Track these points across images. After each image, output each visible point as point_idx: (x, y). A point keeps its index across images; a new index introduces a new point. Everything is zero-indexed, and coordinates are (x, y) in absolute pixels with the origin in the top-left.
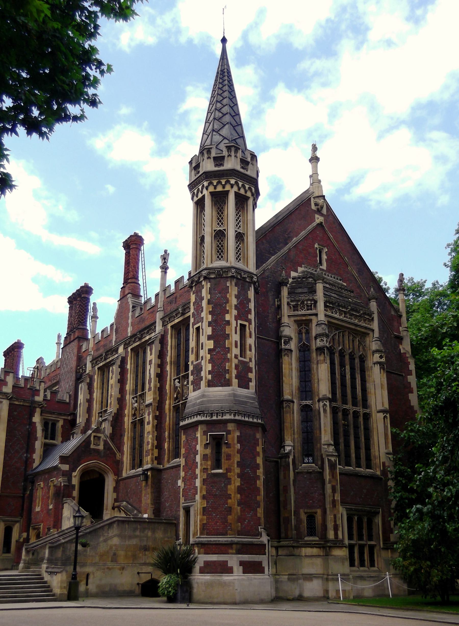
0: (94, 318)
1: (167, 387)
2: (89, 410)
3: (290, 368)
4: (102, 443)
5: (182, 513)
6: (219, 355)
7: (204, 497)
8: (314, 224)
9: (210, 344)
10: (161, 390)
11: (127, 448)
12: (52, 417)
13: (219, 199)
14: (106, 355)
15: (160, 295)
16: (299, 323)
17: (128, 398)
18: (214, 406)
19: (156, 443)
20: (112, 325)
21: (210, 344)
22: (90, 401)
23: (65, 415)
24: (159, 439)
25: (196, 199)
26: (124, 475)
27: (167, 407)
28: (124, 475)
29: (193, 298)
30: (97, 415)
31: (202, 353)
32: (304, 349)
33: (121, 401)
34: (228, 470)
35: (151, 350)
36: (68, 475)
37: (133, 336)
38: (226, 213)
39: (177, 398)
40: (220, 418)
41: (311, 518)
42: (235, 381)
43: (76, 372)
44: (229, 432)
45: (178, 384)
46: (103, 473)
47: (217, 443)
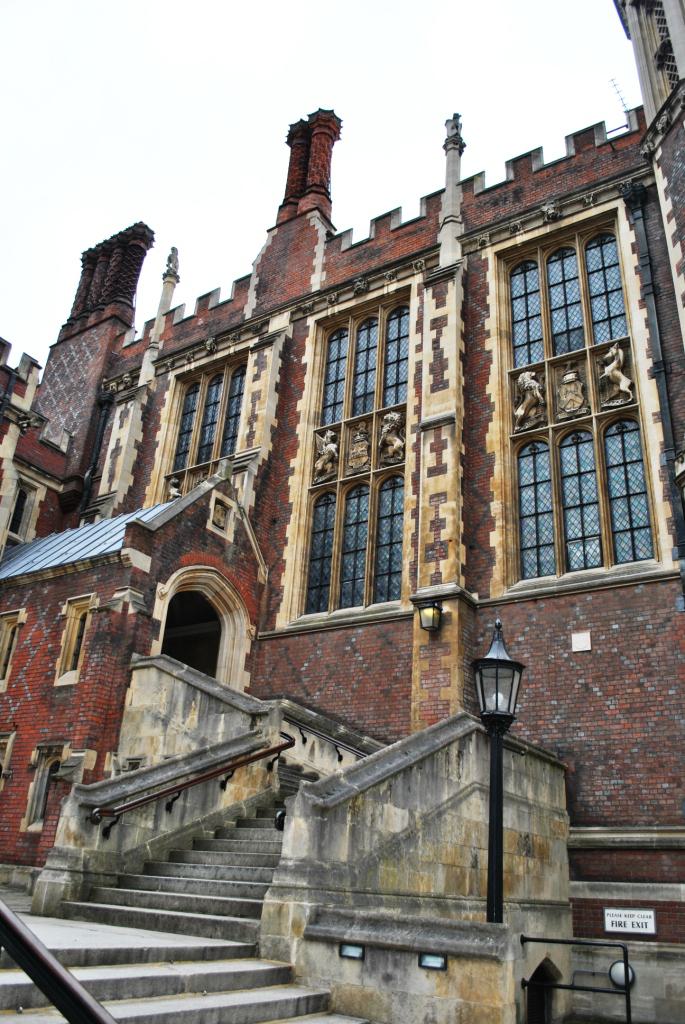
0: (171, 276)
2: (141, 469)
4: (231, 526)
11: (294, 553)
14: (216, 343)
15: (444, 197)
17: (304, 431)
22: (145, 449)
23: (53, 478)
26: (282, 622)
28: (282, 622)
30: (163, 481)
36: (146, 585)
37: (330, 292)
43: (99, 388)
46: (220, 608)
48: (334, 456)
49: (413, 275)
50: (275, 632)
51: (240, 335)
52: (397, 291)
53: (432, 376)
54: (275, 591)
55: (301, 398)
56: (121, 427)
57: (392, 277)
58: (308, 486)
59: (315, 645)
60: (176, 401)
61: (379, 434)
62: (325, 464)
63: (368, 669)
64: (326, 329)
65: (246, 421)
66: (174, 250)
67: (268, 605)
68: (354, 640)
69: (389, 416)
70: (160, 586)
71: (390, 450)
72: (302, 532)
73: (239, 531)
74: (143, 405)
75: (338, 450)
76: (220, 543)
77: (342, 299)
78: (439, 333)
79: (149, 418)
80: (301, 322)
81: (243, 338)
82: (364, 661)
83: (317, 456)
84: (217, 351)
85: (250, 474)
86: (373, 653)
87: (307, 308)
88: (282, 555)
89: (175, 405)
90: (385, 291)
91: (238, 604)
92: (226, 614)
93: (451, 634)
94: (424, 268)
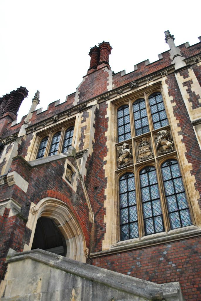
0: (36, 99)
14: (58, 117)
17: (110, 145)
26: (107, 245)
28: (107, 245)
36: (25, 201)
46: (67, 234)
48: (129, 154)
49: (162, 77)
50: (103, 252)
51: (71, 113)
52: (154, 85)
53: (191, 103)
54: (100, 227)
55: (107, 131)
56: (7, 153)
57: (150, 80)
58: (115, 169)
59: (135, 259)
60: (36, 144)
61: (156, 143)
62: (124, 159)
63: (182, 273)
64: (116, 105)
65: (79, 139)
66: (38, 91)
67: (96, 235)
68: (165, 253)
69: (161, 132)
70: (33, 205)
71: (164, 147)
72: (114, 193)
73: (79, 187)
74: (19, 145)
75: (131, 152)
76: (70, 190)
77: (124, 92)
78: (189, 87)
80: (103, 103)
81: (72, 114)
82: (177, 267)
83: (118, 154)
84: (59, 121)
85: (84, 159)
86: (183, 261)
87: (106, 97)
88: (103, 205)
89: (35, 145)
90: (147, 85)
91: (79, 232)
92: (70, 238)
94: (167, 74)
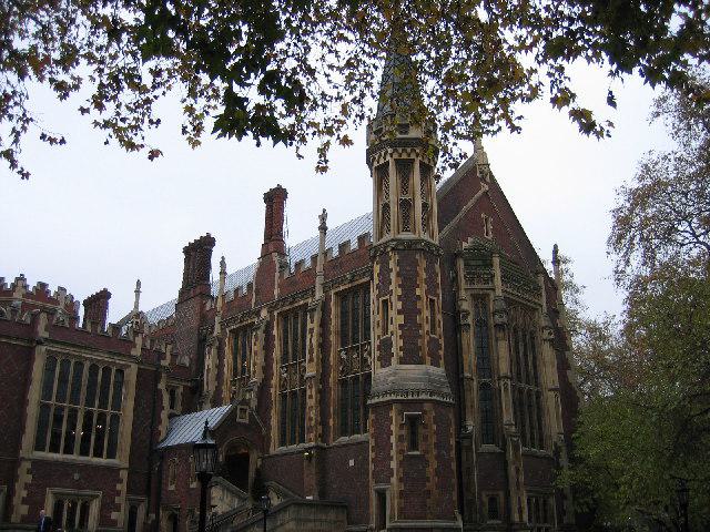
1: (331, 359)
3: (469, 340)
5: (373, 496)
6: (410, 329)
7: (400, 480)
8: (480, 193)
9: (401, 319)
10: (324, 361)
12: (175, 383)
13: (404, 167)
16: (475, 297)
17: (276, 367)
18: (411, 385)
19: (319, 419)
20: (250, 286)
21: (401, 319)
22: (220, 367)
24: (324, 415)
25: (376, 164)
27: (331, 380)
28: (272, 451)
29: (377, 268)
31: (391, 328)
32: (481, 324)
33: (267, 369)
34: (426, 452)
35: (312, 318)
37: (283, 300)
38: (411, 182)
39: (343, 371)
40: (415, 397)
41: (492, 500)
42: (428, 359)
43: (199, 334)
44: (425, 412)
45: (344, 356)
47: (413, 423)
66: (223, 258)
79: (220, 350)
93: (314, 461)
